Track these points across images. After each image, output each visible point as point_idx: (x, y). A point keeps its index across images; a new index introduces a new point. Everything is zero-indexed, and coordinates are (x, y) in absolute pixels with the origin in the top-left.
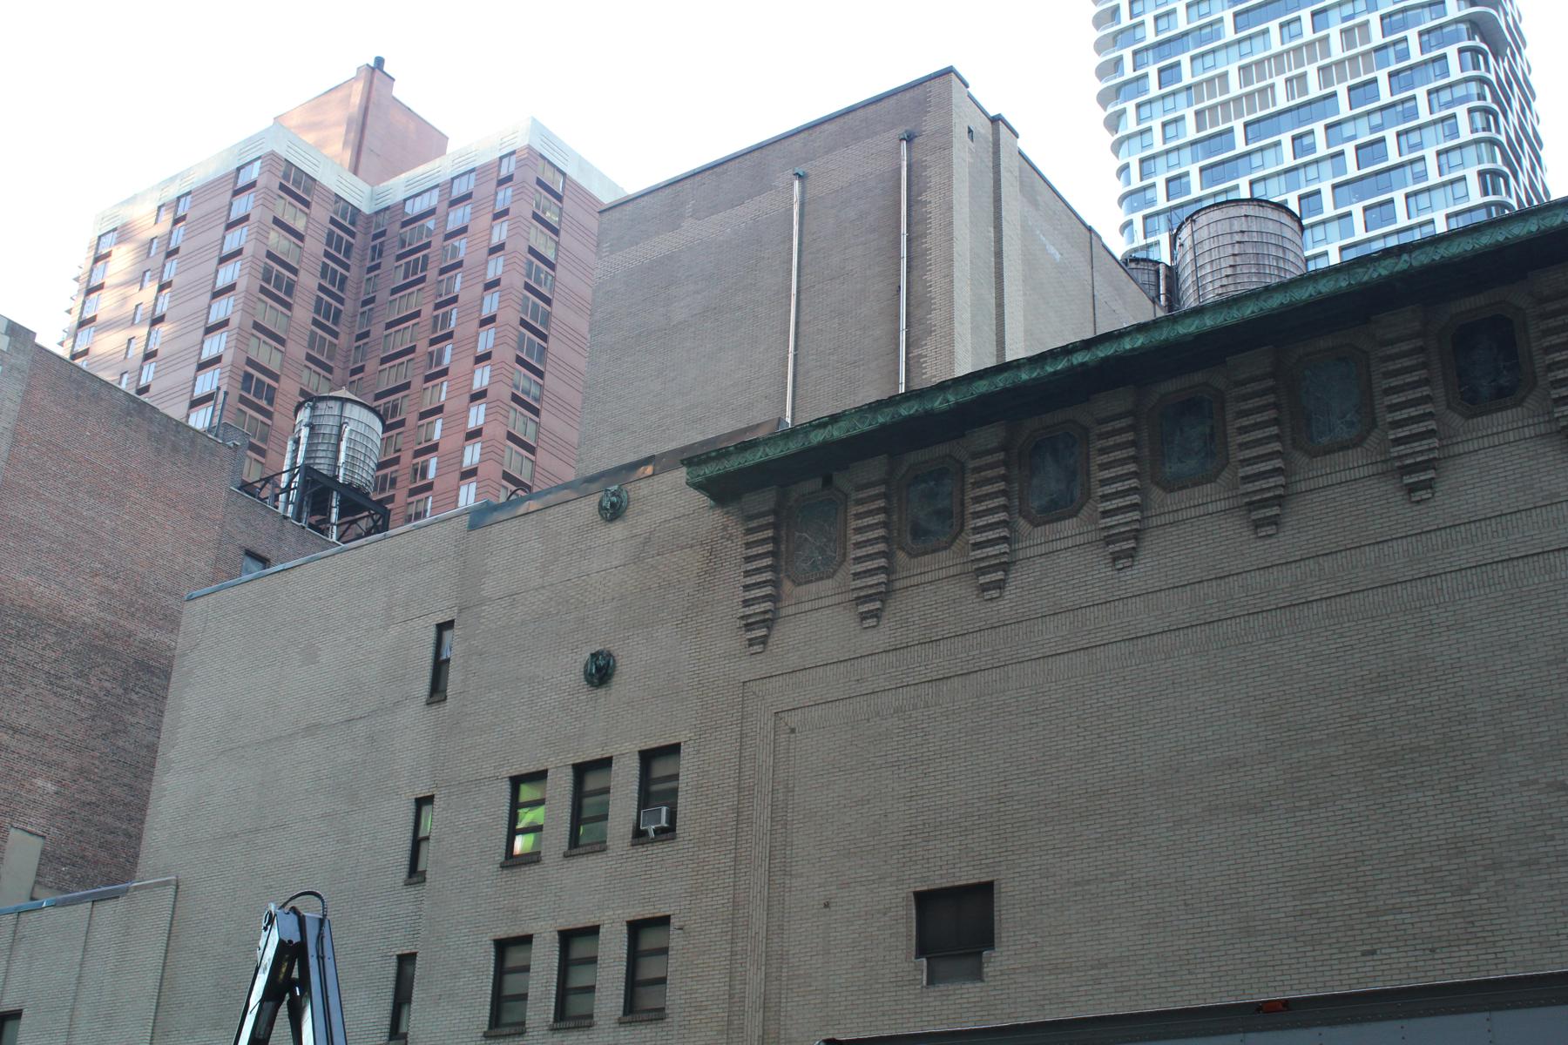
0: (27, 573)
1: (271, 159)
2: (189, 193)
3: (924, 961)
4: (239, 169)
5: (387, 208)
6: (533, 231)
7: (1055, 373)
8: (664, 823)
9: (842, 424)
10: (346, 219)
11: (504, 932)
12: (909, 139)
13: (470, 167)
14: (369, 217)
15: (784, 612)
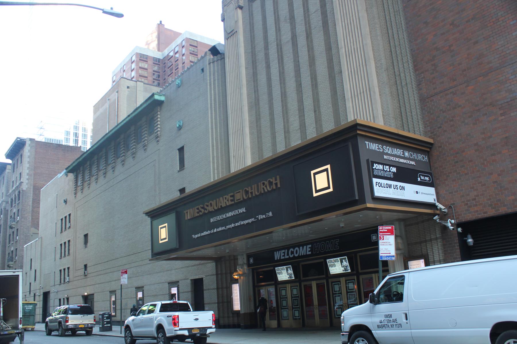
0: (42, 181)
1: (137, 54)
2: (125, 65)
3: (84, 245)
4: (132, 58)
5: (165, 57)
6: (190, 57)
7: (87, 154)
8: (69, 226)
9: (75, 163)
10: (157, 62)
11: (60, 243)
12: (117, 92)
13: (177, 45)
14: (162, 60)
15: (77, 192)
